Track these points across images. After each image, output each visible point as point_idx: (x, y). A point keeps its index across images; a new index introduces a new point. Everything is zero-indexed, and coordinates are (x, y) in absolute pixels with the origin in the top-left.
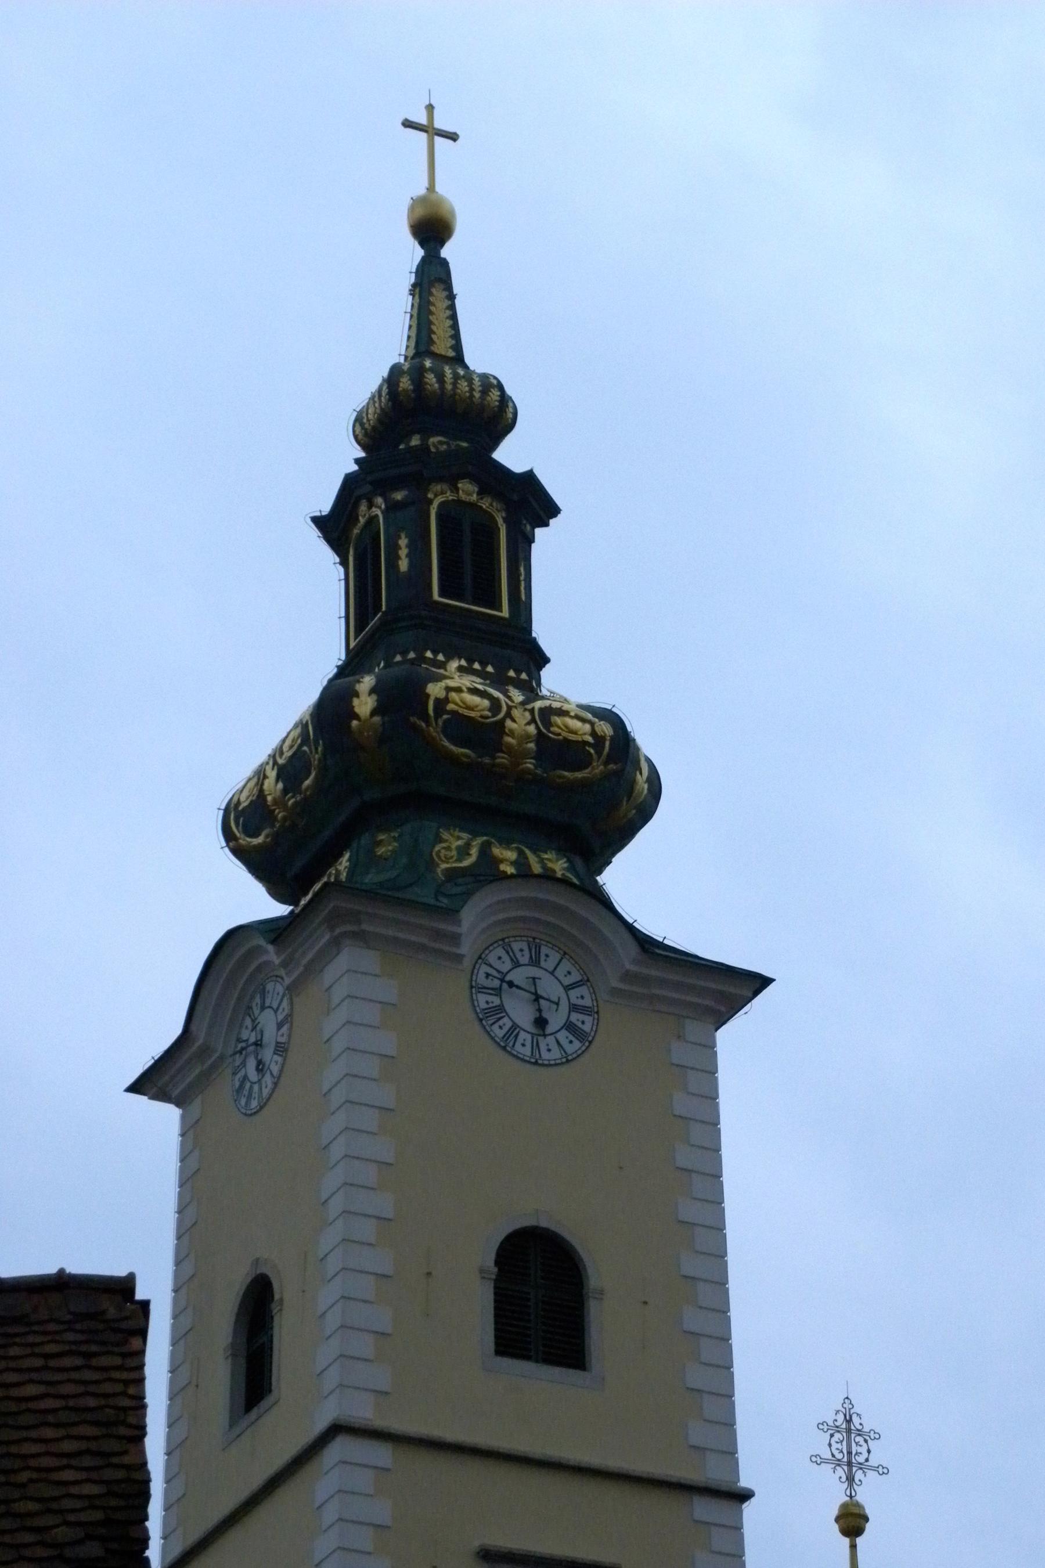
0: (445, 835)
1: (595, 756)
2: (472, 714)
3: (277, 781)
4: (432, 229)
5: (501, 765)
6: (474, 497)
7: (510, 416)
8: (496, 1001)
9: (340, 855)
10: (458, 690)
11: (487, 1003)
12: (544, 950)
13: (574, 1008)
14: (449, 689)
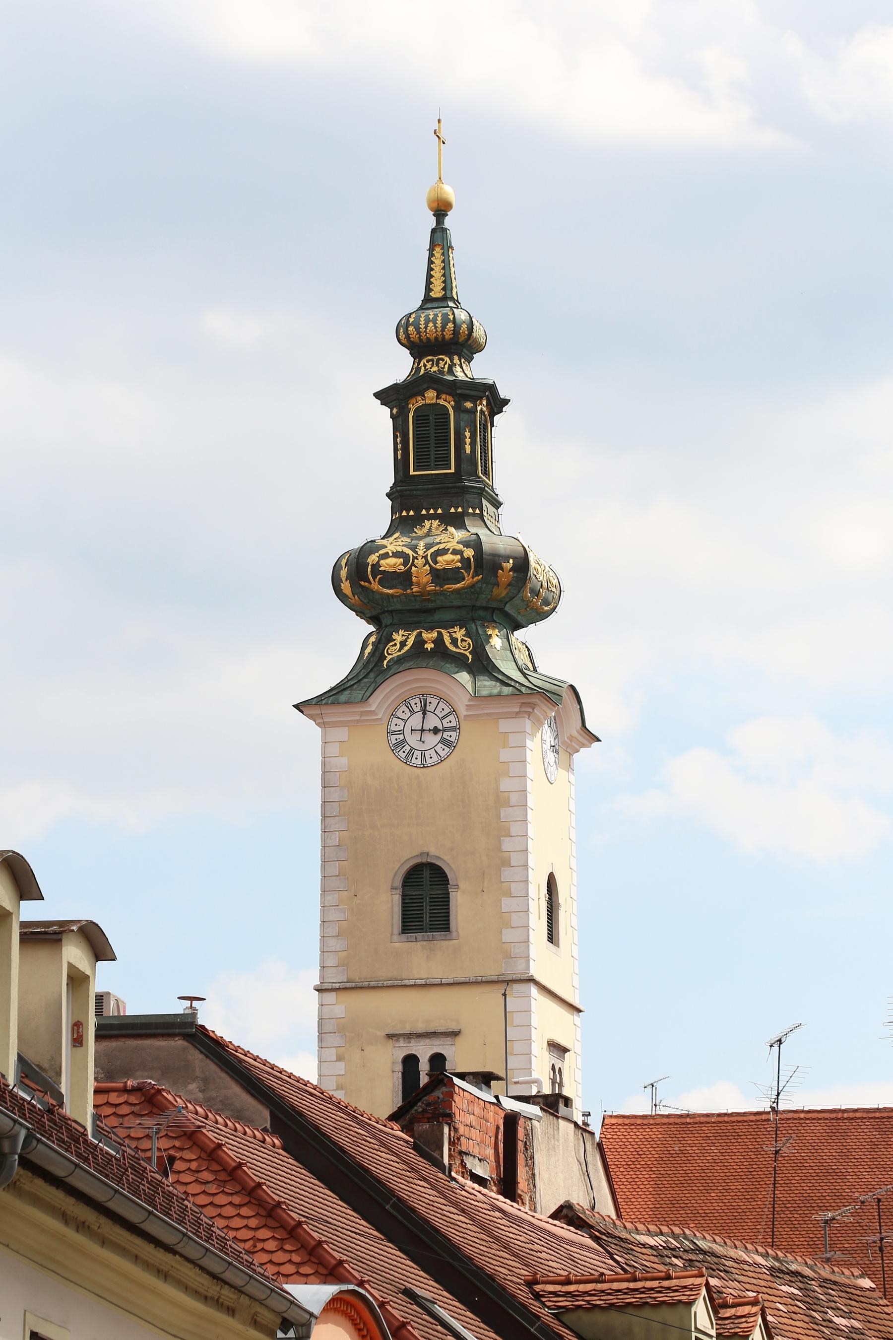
8: (401, 737)
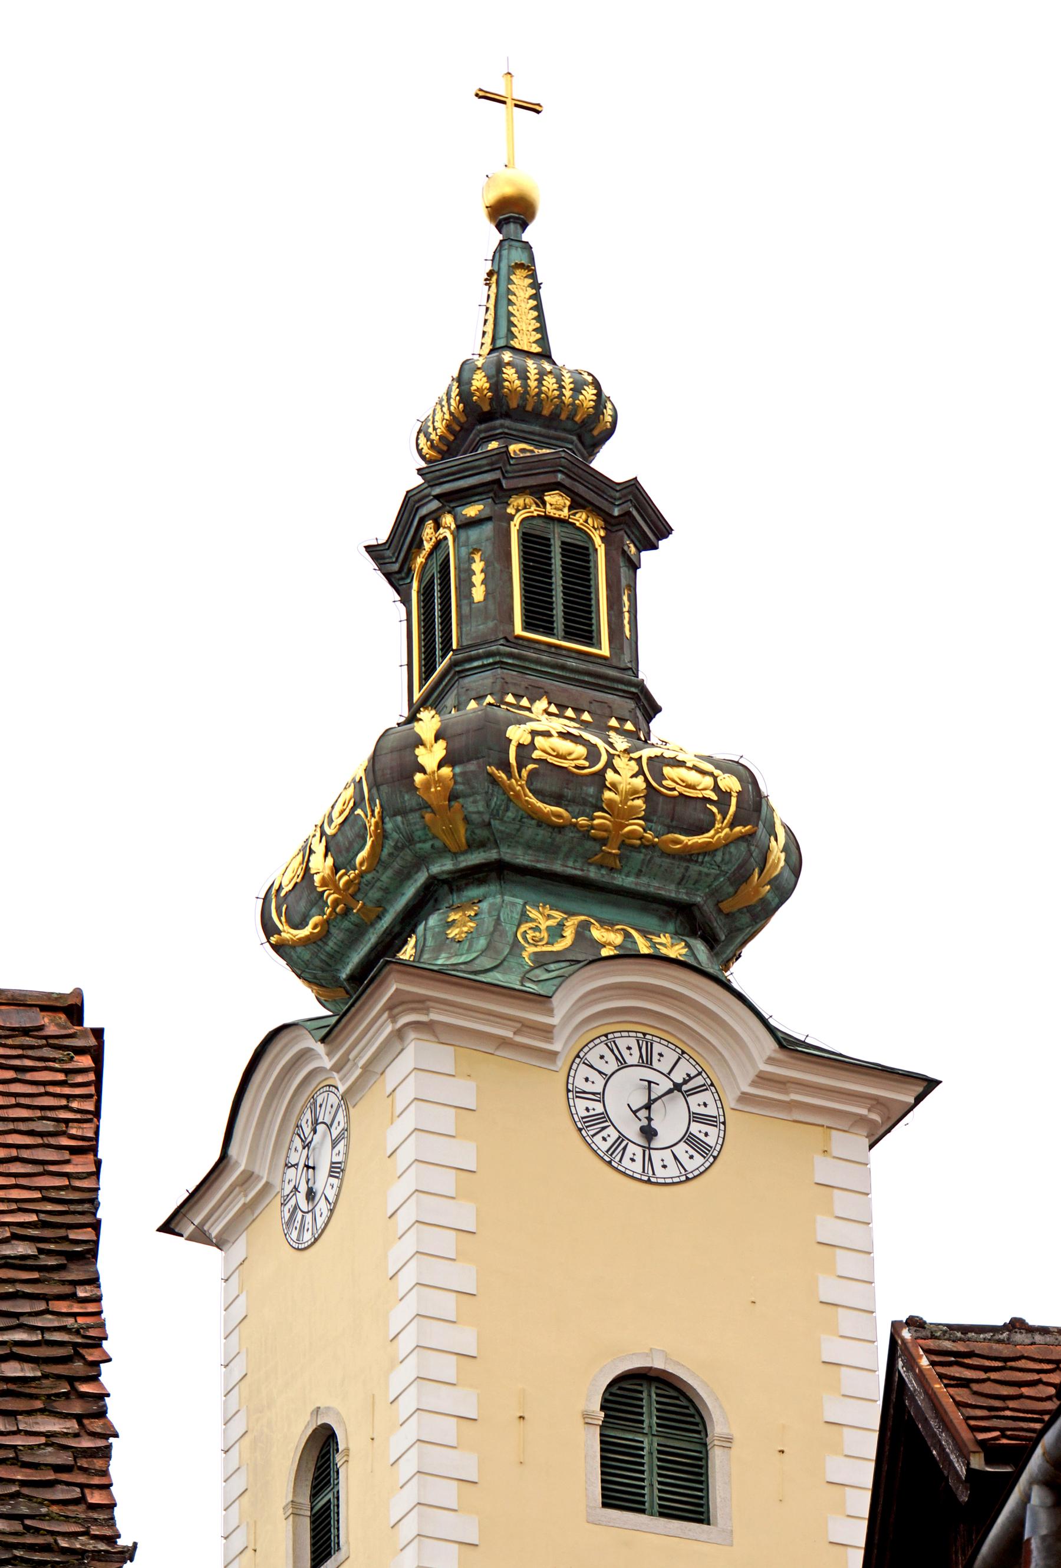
0: (533, 913)
1: (719, 817)
2: (565, 764)
3: (326, 855)
4: (512, 214)
5: (600, 828)
6: (565, 513)
7: (609, 419)
8: (599, 1108)
9: (405, 942)
10: (547, 734)
11: (587, 1110)
12: (657, 1048)
13: (694, 1117)
14: (534, 733)
